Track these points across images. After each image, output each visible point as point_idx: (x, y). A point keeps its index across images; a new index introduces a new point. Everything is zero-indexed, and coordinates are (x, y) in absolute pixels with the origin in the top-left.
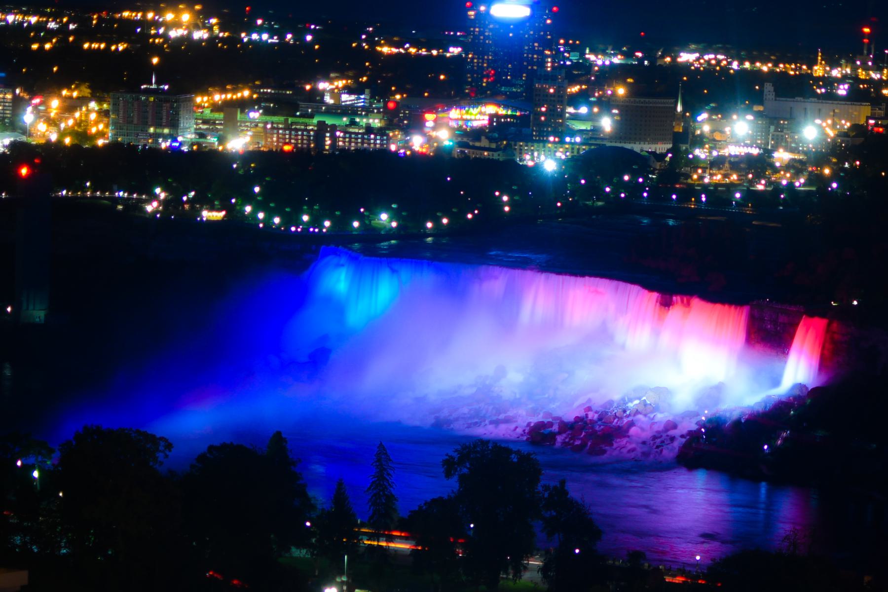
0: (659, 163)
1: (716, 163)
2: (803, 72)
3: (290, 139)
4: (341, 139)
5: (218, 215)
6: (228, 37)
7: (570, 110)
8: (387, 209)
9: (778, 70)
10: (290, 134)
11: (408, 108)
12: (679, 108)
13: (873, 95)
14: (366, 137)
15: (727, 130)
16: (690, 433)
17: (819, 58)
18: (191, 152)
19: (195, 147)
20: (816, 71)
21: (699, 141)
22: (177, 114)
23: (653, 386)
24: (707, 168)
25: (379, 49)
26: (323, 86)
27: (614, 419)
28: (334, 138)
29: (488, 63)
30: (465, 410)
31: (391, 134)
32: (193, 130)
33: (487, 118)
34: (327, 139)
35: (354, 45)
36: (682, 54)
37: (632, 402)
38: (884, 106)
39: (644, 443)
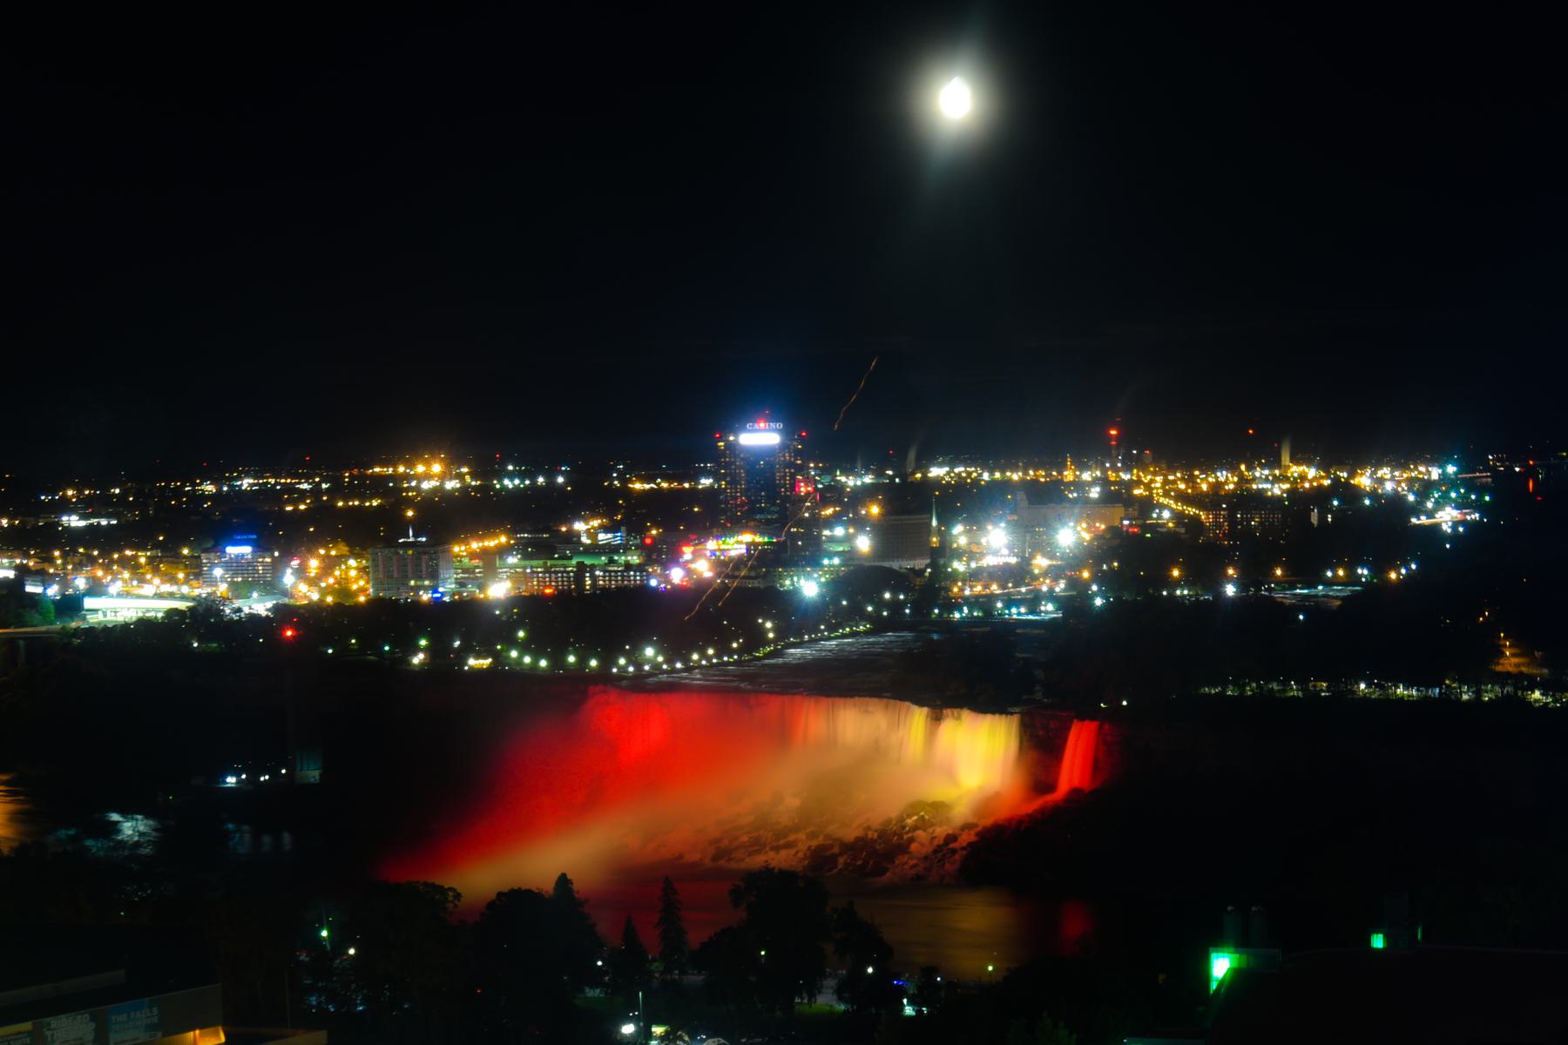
0: (919, 579)
1: (973, 576)
2: (1053, 479)
3: (550, 581)
4: (601, 578)
5: (486, 663)
6: (480, 485)
7: (826, 532)
8: (651, 643)
9: (1029, 478)
10: (550, 577)
11: (665, 543)
12: (934, 523)
13: (1125, 496)
14: (625, 574)
15: (983, 541)
16: (970, 844)
17: (1069, 463)
18: (453, 603)
19: (456, 597)
20: (1066, 476)
21: (958, 554)
22: (437, 565)
23: (929, 802)
24: (966, 580)
25: (631, 486)
26: (579, 526)
27: (894, 836)
28: (593, 578)
29: (741, 492)
30: (745, 839)
31: (650, 570)
32: (453, 580)
33: (744, 546)
34: (587, 579)
35: (606, 484)
36: (931, 469)
37: (910, 818)
38: (1136, 507)
39: (926, 858)
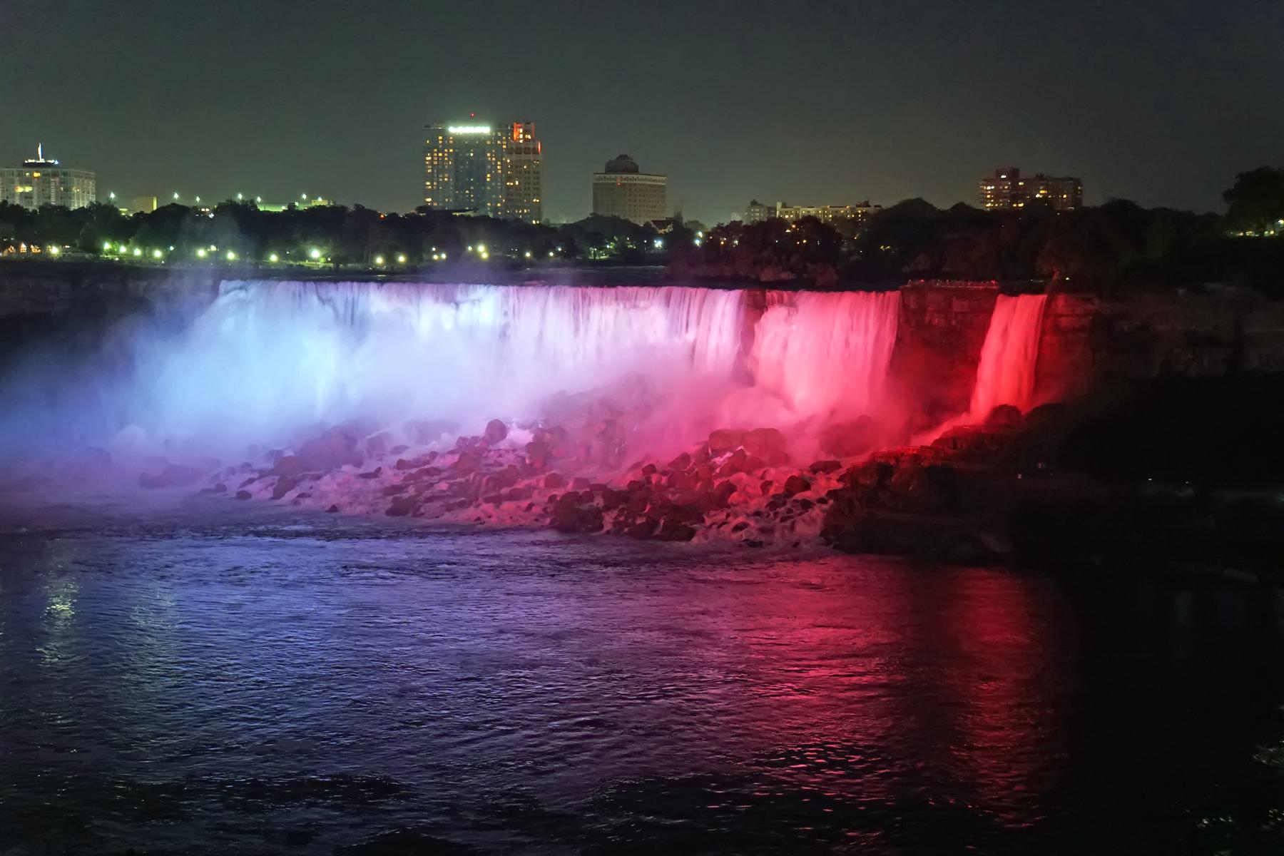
27: (697, 482)
30: (443, 486)
